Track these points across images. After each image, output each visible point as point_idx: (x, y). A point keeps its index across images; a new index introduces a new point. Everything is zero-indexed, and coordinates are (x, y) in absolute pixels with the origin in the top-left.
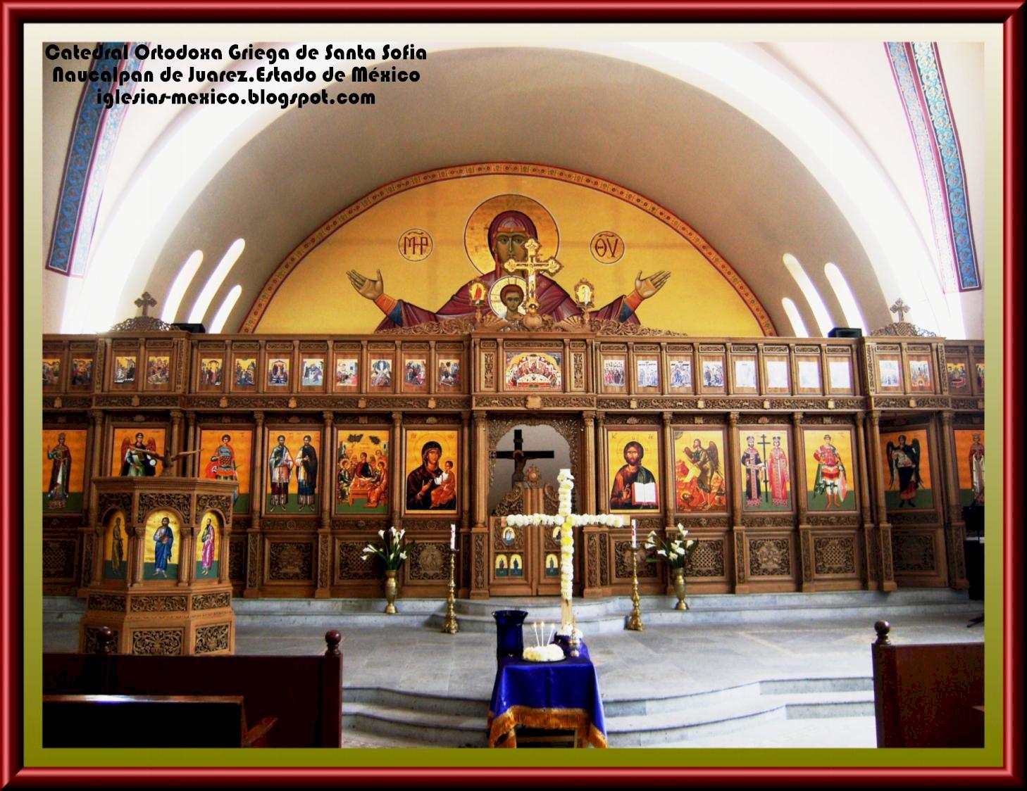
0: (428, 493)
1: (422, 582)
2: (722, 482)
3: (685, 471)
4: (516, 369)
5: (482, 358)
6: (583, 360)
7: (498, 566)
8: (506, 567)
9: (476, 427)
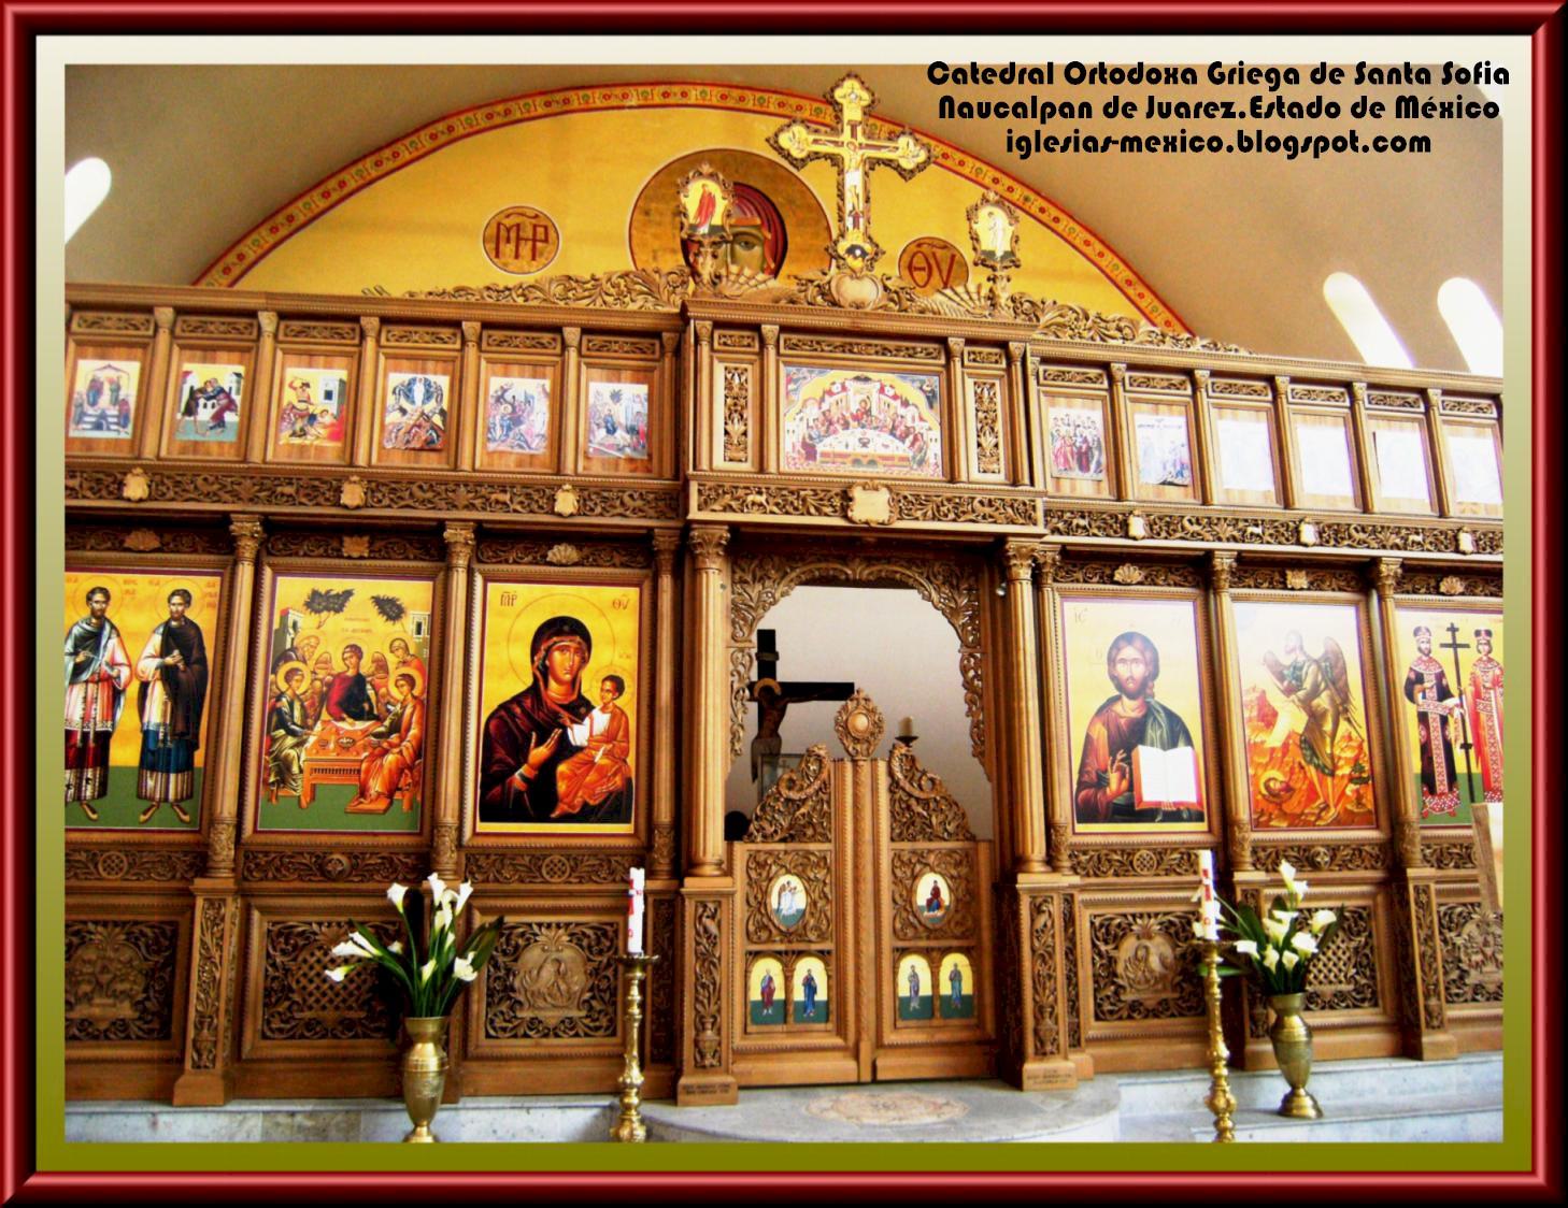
0: (547, 768)
1: (521, 1046)
2: (1360, 747)
3: (1268, 718)
4: (813, 412)
5: (716, 379)
6: (998, 399)
7: (756, 995)
8: (779, 995)
9: (696, 572)
